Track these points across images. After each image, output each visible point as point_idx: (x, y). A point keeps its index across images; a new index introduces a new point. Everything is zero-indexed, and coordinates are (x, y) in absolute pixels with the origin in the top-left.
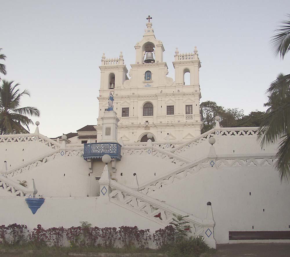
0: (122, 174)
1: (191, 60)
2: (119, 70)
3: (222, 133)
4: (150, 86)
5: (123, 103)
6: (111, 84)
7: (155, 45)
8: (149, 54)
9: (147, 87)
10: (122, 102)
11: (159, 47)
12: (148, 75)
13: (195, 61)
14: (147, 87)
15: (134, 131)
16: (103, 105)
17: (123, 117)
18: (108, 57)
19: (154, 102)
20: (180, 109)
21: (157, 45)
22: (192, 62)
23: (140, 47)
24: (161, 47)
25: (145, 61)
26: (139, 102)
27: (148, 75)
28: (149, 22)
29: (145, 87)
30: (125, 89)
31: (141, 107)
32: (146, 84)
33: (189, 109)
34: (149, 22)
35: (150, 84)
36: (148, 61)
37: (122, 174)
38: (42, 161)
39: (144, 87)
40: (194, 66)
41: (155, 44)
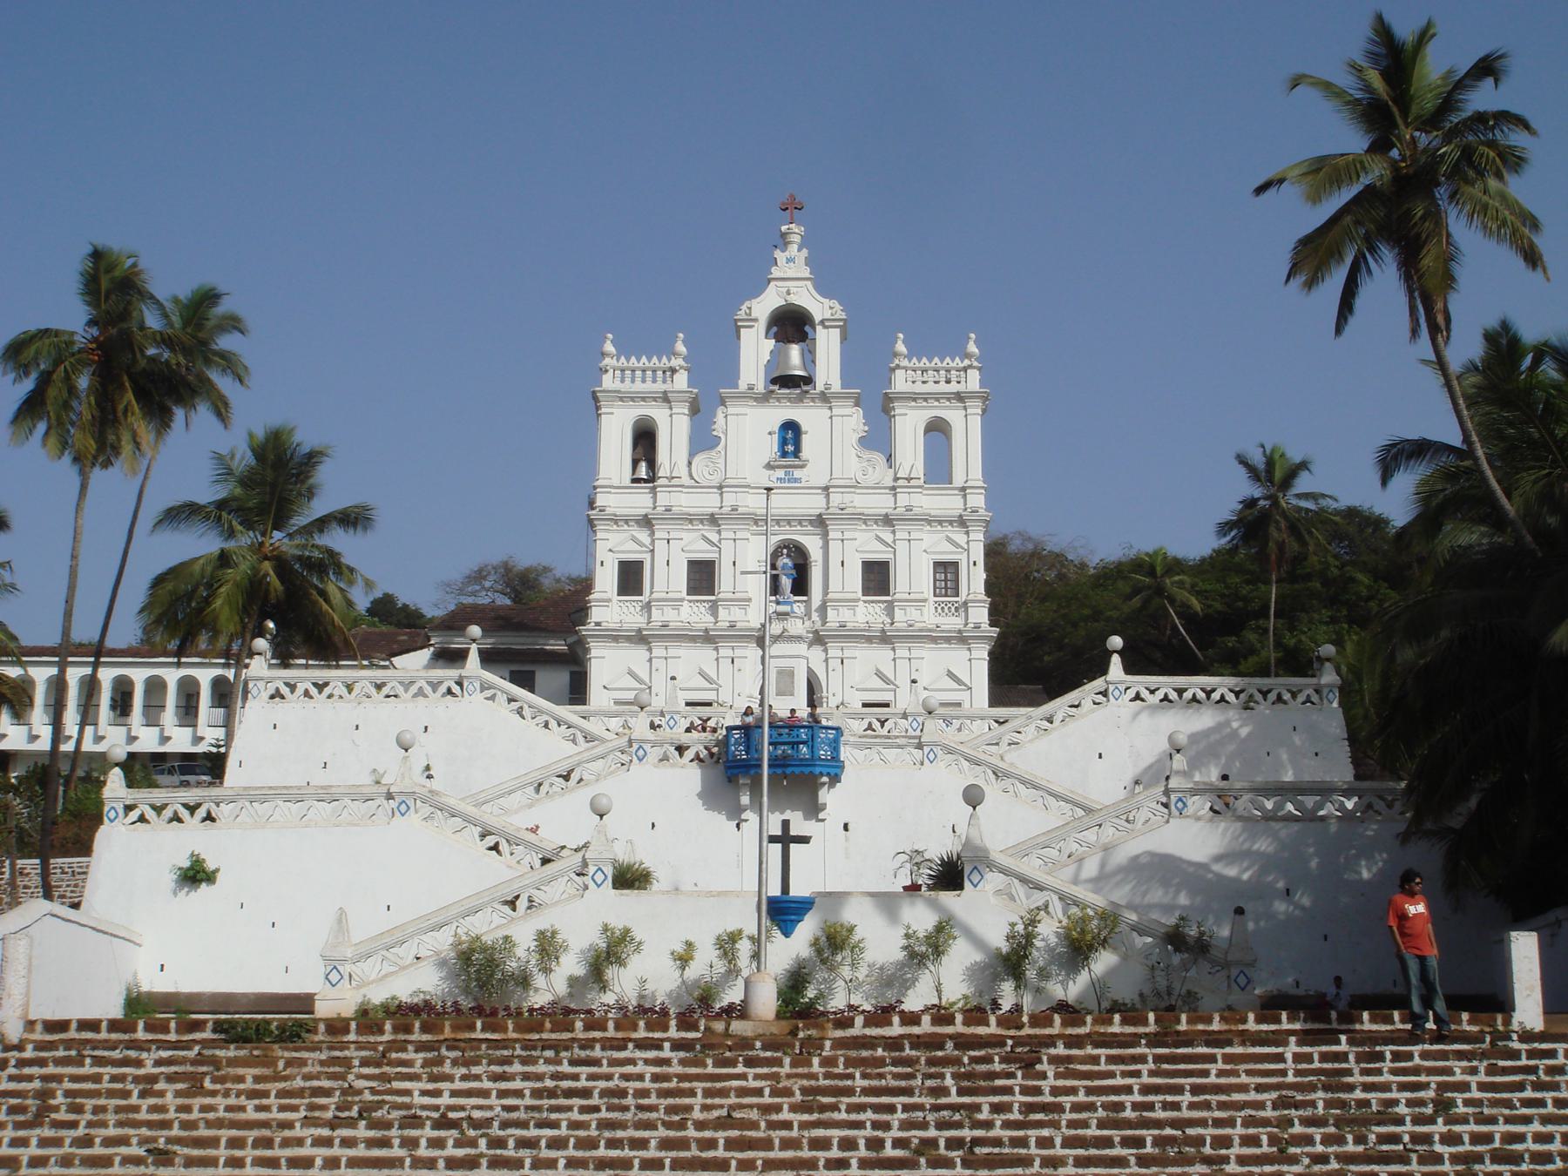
0: (846, 827)
1: (953, 387)
3: (1131, 693)
4: (796, 480)
6: (635, 463)
7: (817, 318)
8: (795, 351)
13: (972, 395)
15: (738, 652)
16: (609, 545)
19: (812, 544)
20: (913, 578)
21: (822, 322)
22: (960, 397)
23: (756, 320)
24: (838, 330)
25: (774, 381)
30: (697, 485)
32: (780, 473)
33: (947, 573)
35: (797, 473)
36: (786, 381)
37: (846, 827)
38: (566, 778)
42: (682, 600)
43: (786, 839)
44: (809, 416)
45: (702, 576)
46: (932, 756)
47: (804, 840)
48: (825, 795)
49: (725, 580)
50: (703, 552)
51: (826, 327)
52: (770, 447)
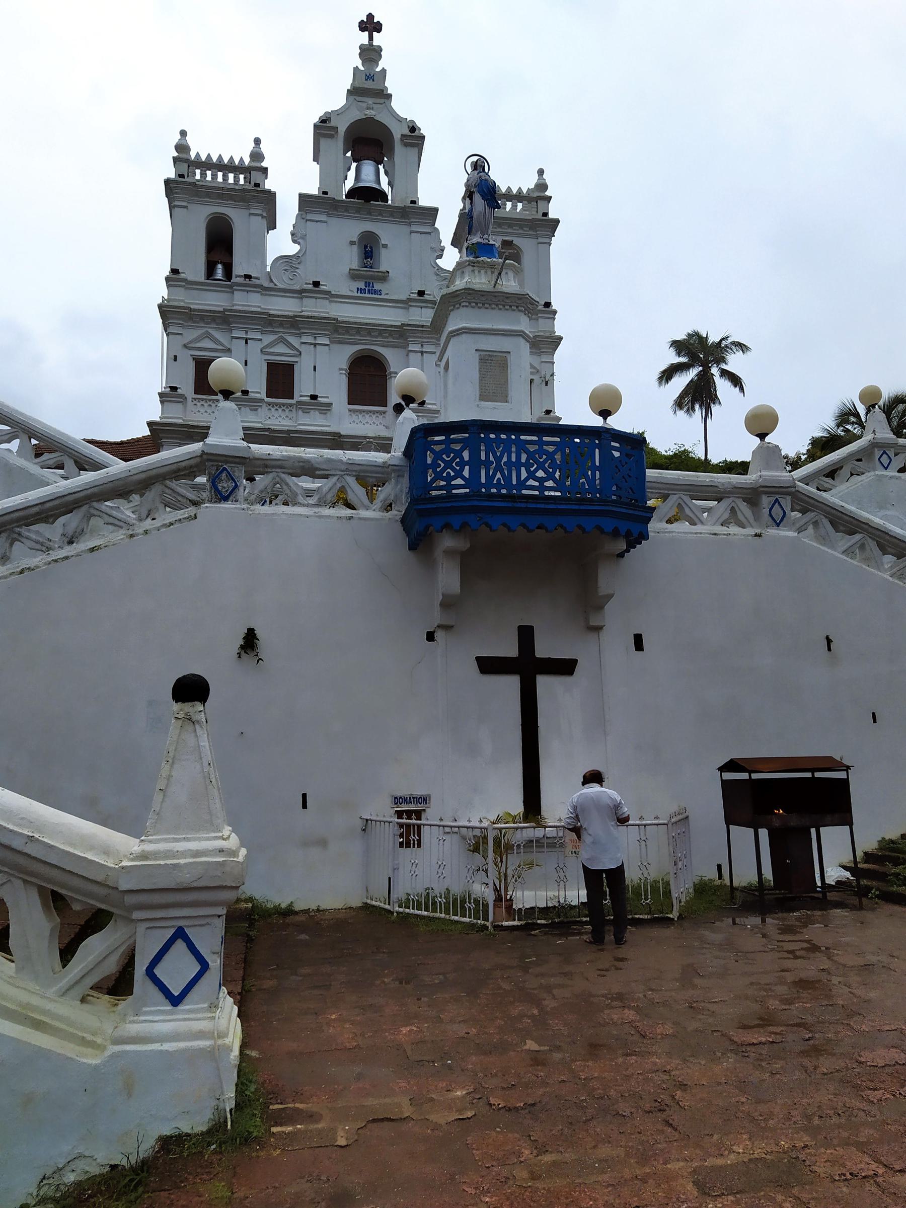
2: (252, 211)
4: (375, 292)
5: (271, 345)
7: (397, 136)
9: (366, 295)
10: (268, 339)
11: (409, 149)
12: (369, 248)
14: (366, 295)
16: (186, 342)
17: (270, 400)
18: (199, 148)
19: (390, 355)
25: (352, 193)
26: (335, 347)
27: (369, 248)
28: (371, 38)
29: (356, 294)
31: (341, 369)
34: (371, 38)
39: (350, 294)
40: (535, 241)
41: (398, 132)
42: (261, 400)
43: (527, 667)
44: (386, 232)
45: (281, 380)
46: (777, 512)
47: (566, 667)
48: (607, 579)
49: (303, 387)
50: (281, 354)
51: (406, 145)
52: (352, 259)
